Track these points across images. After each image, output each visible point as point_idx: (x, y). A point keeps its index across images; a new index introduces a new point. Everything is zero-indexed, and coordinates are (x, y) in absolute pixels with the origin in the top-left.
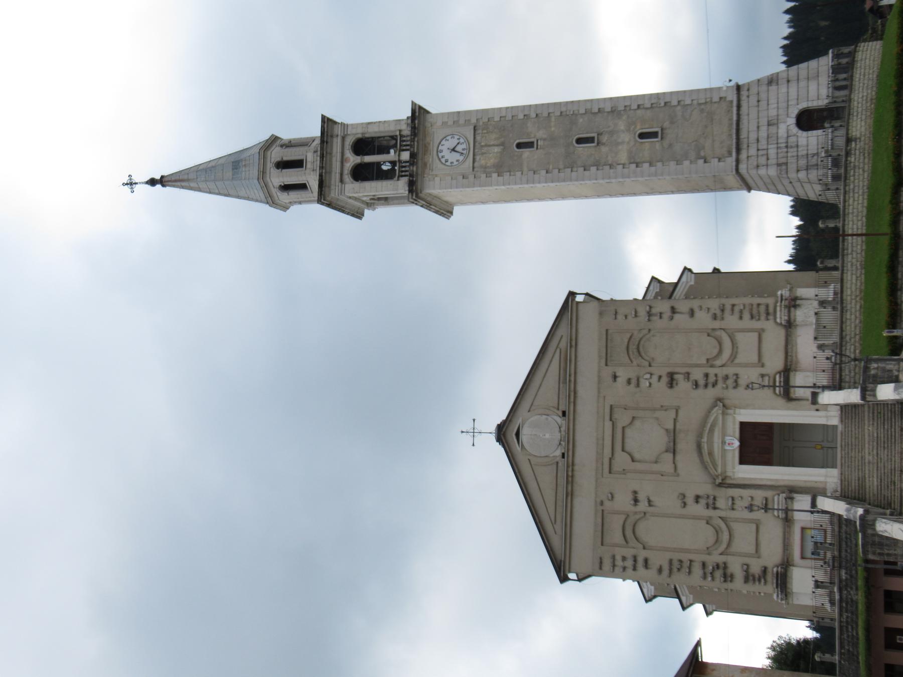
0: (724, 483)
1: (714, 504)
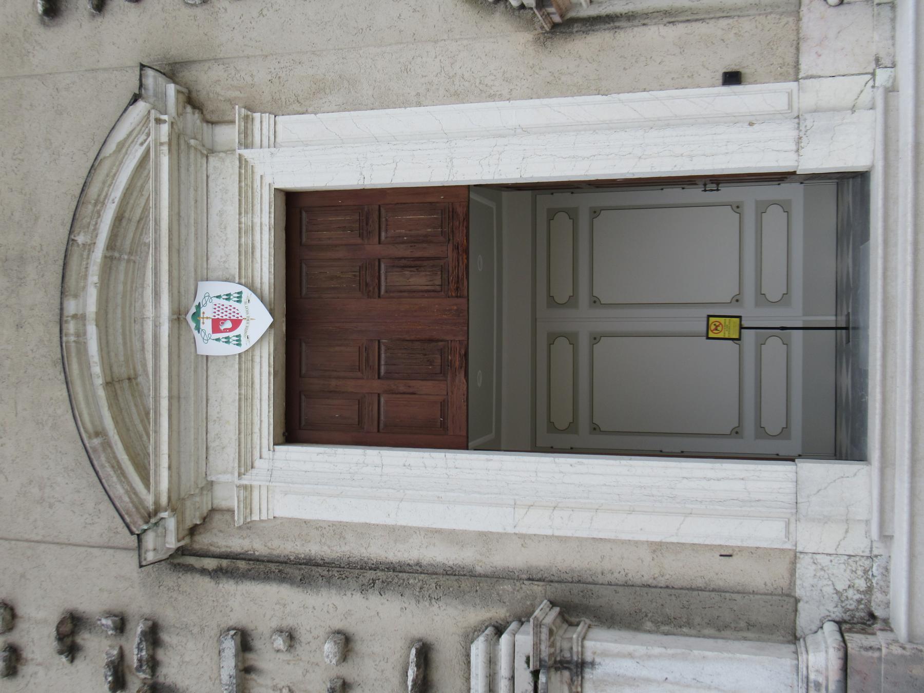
0: (198, 551)
1: (153, 664)
